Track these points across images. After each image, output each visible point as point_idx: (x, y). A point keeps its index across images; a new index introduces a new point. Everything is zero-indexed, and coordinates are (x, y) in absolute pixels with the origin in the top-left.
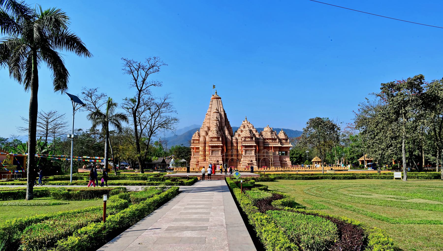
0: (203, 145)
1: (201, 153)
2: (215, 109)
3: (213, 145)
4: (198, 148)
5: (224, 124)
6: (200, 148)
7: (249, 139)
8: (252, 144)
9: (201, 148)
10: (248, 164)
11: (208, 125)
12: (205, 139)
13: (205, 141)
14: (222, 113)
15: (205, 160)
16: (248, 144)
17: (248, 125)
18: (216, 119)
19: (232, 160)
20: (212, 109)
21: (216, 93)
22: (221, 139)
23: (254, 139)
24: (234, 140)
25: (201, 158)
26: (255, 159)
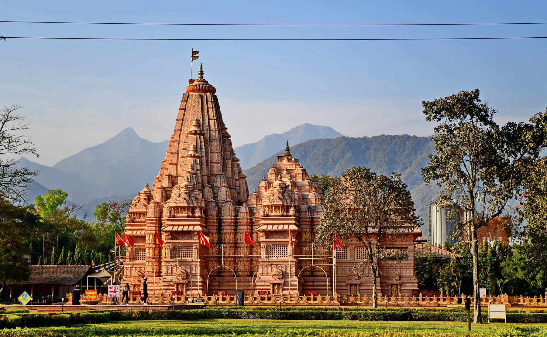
0: (153, 230)
1: (149, 253)
2: (194, 123)
3: (175, 228)
4: (143, 238)
5: (217, 168)
6: (147, 238)
7: (279, 213)
8: (286, 227)
9: (149, 239)
10: (274, 285)
11: (172, 171)
12: (161, 213)
13: (160, 217)
14: (215, 134)
15: (159, 274)
16: (275, 228)
17: (292, 167)
18: (191, 153)
19: (220, 272)
20: (185, 124)
21: (201, 73)
22: (197, 213)
23: (292, 212)
24: (243, 215)
25: (148, 267)
26: (294, 270)
